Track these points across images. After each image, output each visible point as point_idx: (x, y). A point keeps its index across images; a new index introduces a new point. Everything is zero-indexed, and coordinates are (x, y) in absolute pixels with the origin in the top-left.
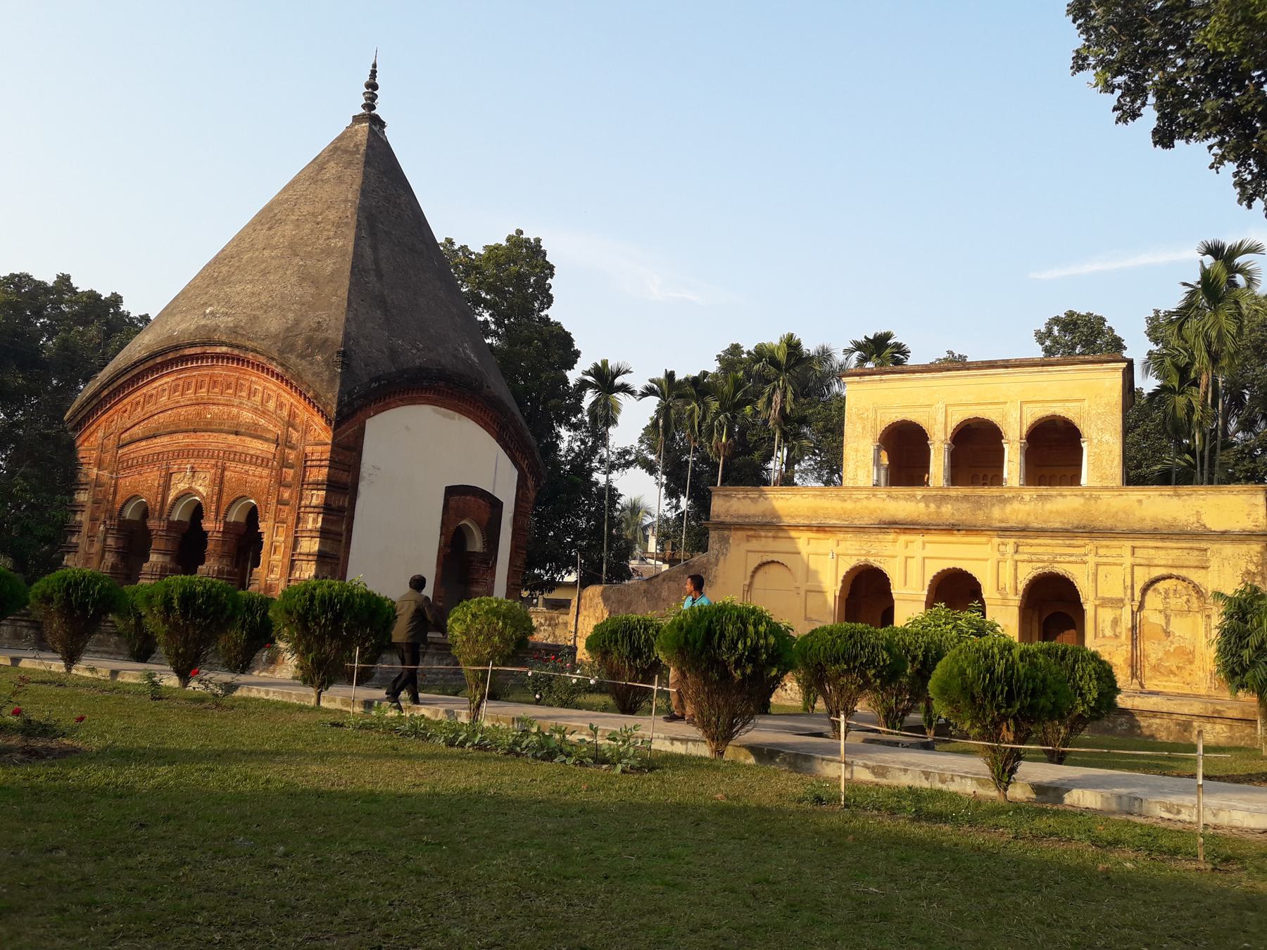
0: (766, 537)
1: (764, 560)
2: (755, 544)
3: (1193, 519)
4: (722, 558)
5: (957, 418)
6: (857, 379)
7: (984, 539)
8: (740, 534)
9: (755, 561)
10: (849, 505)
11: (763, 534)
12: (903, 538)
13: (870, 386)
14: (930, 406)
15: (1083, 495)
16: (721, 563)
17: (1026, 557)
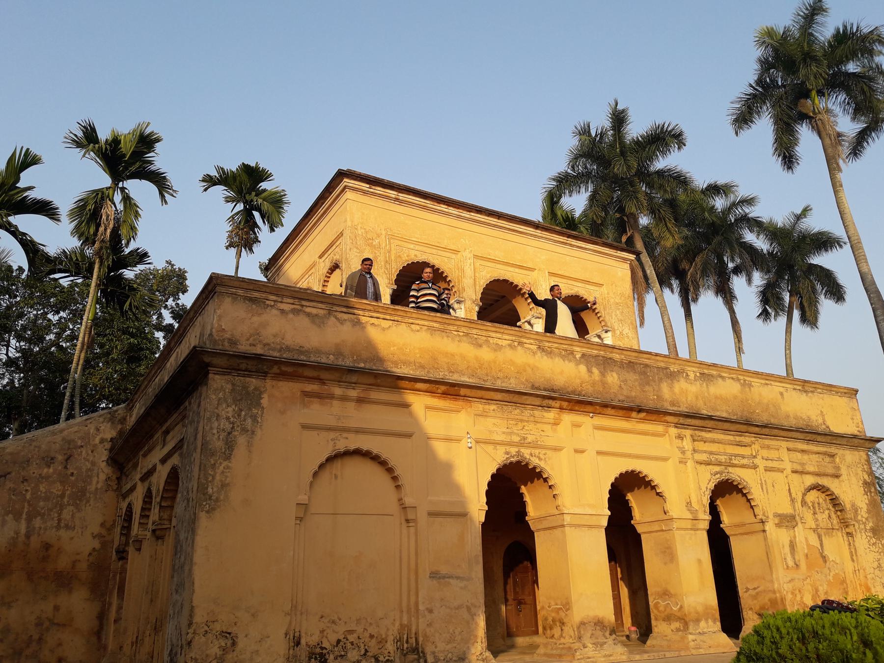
0: (344, 399)
1: (341, 446)
2: (318, 413)
3: (820, 421)
4: (242, 440)
5: (488, 274)
6: (365, 186)
7: (660, 428)
8: (288, 388)
9: (321, 447)
10: (486, 354)
11: (338, 391)
12: (568, 418)
13: (380, 203)
14: (456, 252)
15: (739, 380)
16: (240, 451)
17: (704, 457)
